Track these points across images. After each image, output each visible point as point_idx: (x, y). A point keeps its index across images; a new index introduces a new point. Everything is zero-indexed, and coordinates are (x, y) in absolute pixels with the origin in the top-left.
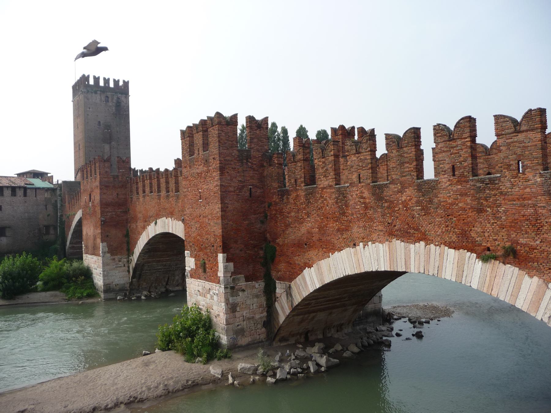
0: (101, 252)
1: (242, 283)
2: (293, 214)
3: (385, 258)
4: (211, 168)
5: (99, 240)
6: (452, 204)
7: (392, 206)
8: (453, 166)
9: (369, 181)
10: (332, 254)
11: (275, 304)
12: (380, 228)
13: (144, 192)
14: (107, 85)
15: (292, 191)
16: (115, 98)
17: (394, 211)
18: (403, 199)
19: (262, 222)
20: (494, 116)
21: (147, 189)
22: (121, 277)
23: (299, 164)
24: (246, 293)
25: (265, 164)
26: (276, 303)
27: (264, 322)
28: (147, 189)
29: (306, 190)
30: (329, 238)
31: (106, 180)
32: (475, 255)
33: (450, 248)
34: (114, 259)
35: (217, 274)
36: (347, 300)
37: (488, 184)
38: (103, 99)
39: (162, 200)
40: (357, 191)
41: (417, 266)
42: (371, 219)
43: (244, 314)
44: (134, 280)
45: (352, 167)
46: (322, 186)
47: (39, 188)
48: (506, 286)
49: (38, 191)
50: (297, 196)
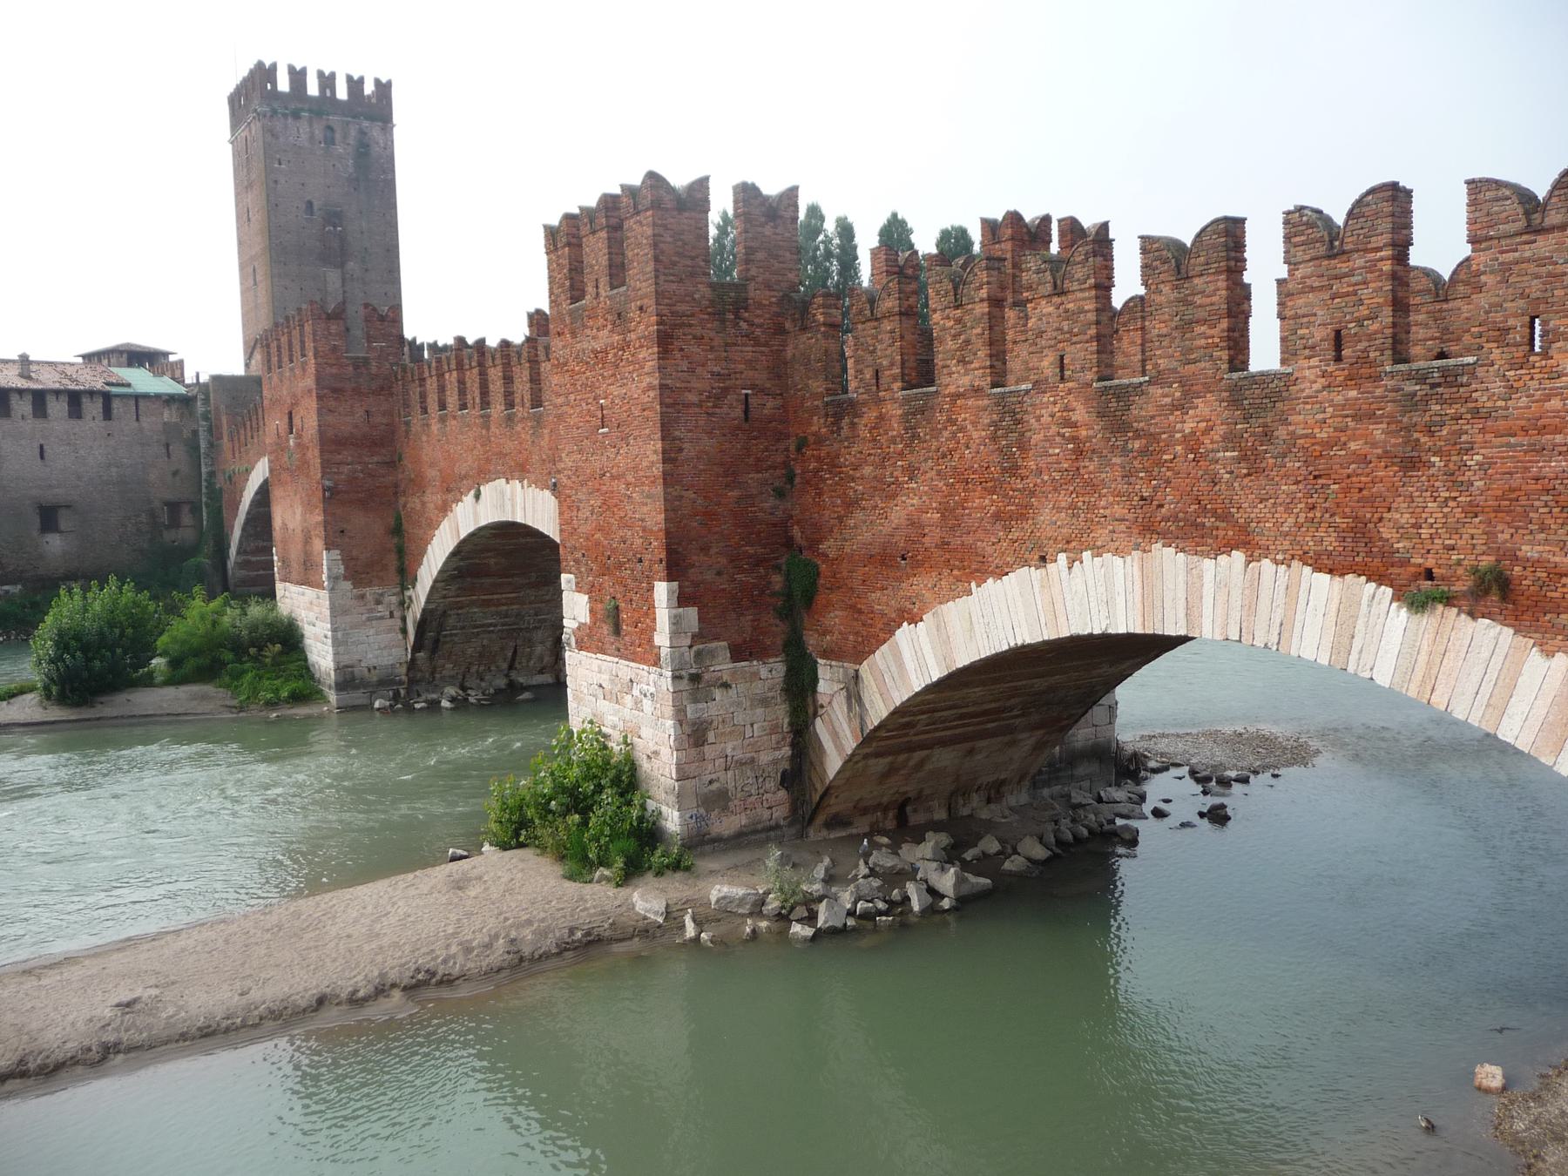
0: (324, 577)
1: (723, 666)
2: (867, 470)
3: (1130, 597)
4: (633, 336)
5: (318, 544)
6: (1329, 444)
7: (1153, 447)
8: (1338, 332)
9: (1090, 376)
10: (979, 586)
11: (813, 723)
12: (1119, 511)
13: (443, 406)
14: (328, 93)
15: (865, 403)
16: (353, 133)
17: (1160, 464)
18: (1188, 427)
19: (780, 494)
20: (1468, 182)
21: (452, 399)
22: (386, 648)
23: (887, 326)
24: (732, 692)
25: (788, 325)
26: (818, 721)
27: (784, 773)
28: (452, 399)
29: (907, 400)
30: (969, 540)
31: (334, 371)
32: (1389, 591)
33: (1318, 569)
34: (362, 597)
35: (650, 640)
36: (1017, 717)
37: (1439, 385)
38: (319, 133)
39: (493, 429)
40: (1055, 403)
41: (1219, 621)
42: (1092, 487)
43: (729, 752)
44: (421, 655)
45: (1040, 334)
46: (952, 389)
47: (146, 396)
48: (1476, 679)
49: (142, 403)
50: (881, 417)
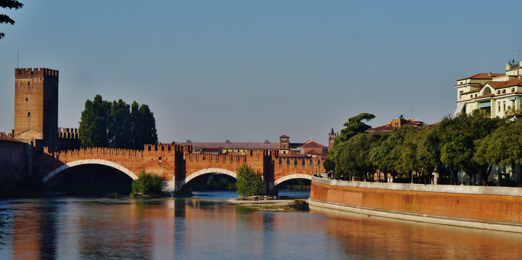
7: (298, 169)
